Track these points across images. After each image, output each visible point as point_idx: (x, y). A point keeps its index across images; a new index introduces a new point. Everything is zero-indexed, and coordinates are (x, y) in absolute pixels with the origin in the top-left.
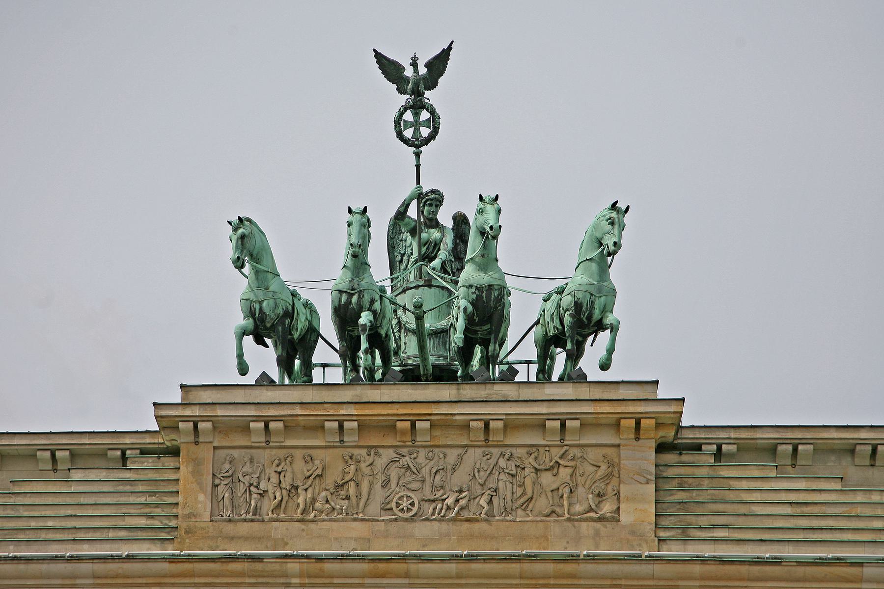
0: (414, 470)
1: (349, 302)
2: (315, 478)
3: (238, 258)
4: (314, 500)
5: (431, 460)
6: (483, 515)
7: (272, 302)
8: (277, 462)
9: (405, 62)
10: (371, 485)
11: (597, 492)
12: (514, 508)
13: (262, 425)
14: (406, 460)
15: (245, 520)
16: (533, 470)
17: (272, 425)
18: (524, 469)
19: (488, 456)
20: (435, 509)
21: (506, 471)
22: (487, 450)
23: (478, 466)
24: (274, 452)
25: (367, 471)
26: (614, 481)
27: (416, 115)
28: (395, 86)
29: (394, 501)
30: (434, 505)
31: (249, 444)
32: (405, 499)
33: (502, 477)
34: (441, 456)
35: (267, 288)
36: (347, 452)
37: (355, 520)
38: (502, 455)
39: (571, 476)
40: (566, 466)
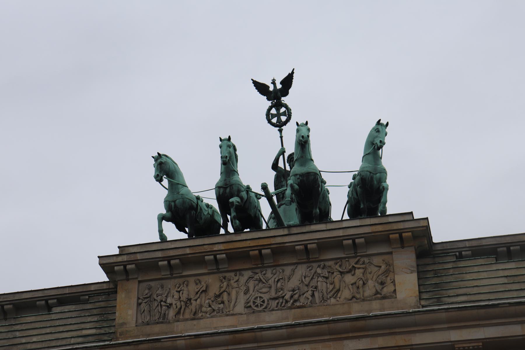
0: (264, 281)
1: (224, 192)
2: (201, 293)
3: (158, 175)
4: (201, 306)
5: (274, 274)
6: (309, 303)
7: (181, 200)
8: (178, 285)
9: (269, 83)
10: (237, 293)
11: (380, 281)
12: (329, 297)
13: (166, 263)
14: (260, 276)
15: (158, 323)
16: (338, 273)
17: (172, 262)
18: (333, 273)
19: (310, 268)
20: (278, 303)
21: (322, 275)
22: (309, 265)
23: (304, 275)
24: (176, 281)
25: (235, 285)
26: (391, 275)
27: (278, 110)
28: (265, 97)
29: (252, 301)
30: (277, 301)
31: (160, 277)
32: (259, 299)
33: (320, 279)
34: (281, 271)
35: (178, 193)
36: (221, 275)
37: (227, 315)
38: (319, 266)
39: (363, 274)
40: (359, 268)
